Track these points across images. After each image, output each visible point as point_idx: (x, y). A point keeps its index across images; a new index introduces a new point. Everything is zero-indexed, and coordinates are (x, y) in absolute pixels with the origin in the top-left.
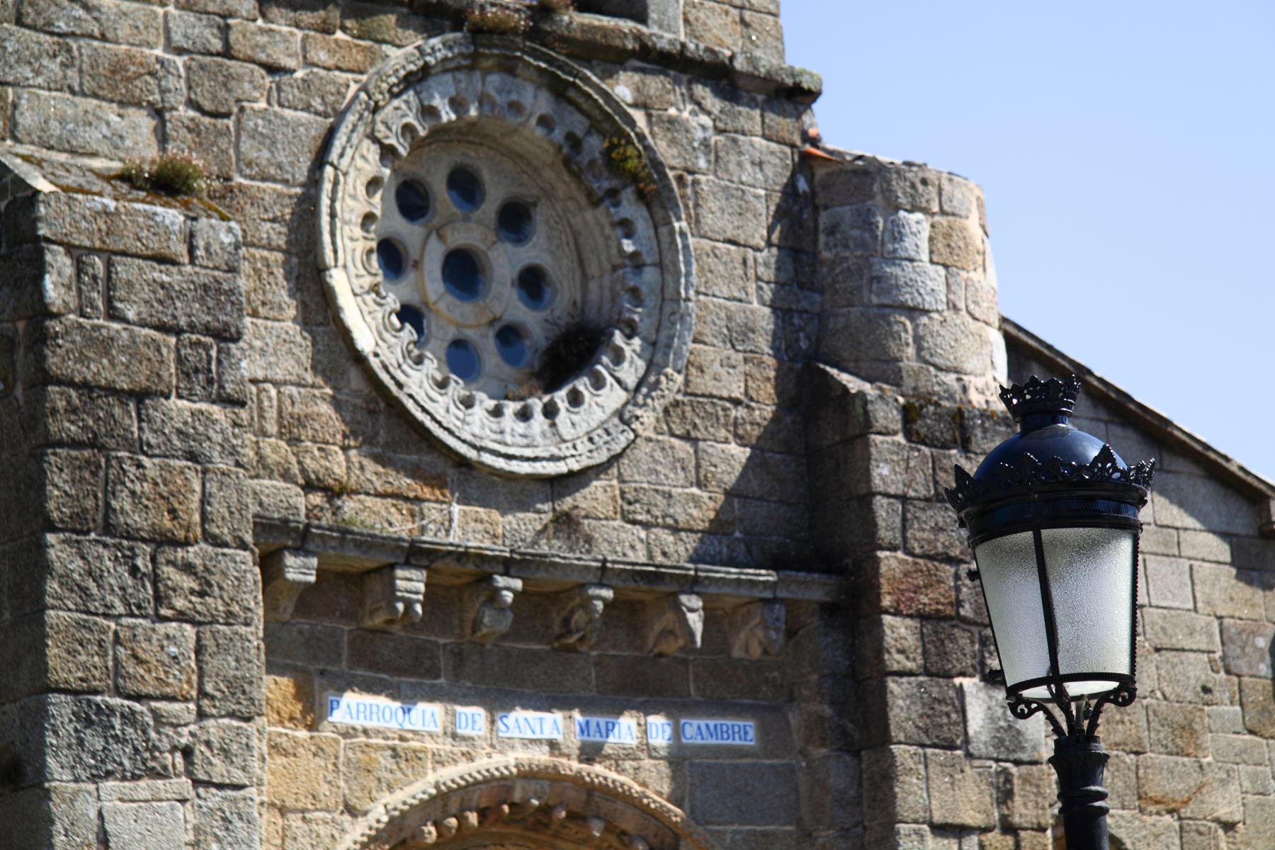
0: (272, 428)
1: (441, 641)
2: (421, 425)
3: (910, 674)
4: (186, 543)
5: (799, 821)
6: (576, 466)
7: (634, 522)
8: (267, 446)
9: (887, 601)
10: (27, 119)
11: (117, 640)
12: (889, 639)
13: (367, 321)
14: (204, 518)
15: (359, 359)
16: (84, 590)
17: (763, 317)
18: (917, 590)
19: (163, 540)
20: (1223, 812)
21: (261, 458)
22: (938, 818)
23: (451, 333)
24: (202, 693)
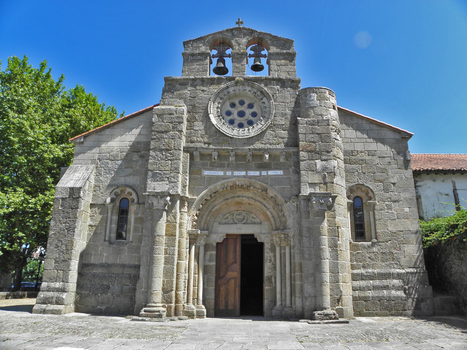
0: (199, 136)
2: (223, 133)
3: (305, 160)
4: (170, 150)
5: (291, 185)
6: (250, 136)
7: (263, 144)
8: (198, 139)
9: (301, 149)
10: (166, 102)
11: (159, 164)
12: (301, 155)
13: (214, 120)
14: (174, 147)
15: (214, 125)
16: (155, 158)
17: (289, 112)
18: (307, 147)
19: (167, 150)
20: (393, 181)
21: (197, 140)
22: (310, 182)
23: (239, 122)
24: (171, 170)
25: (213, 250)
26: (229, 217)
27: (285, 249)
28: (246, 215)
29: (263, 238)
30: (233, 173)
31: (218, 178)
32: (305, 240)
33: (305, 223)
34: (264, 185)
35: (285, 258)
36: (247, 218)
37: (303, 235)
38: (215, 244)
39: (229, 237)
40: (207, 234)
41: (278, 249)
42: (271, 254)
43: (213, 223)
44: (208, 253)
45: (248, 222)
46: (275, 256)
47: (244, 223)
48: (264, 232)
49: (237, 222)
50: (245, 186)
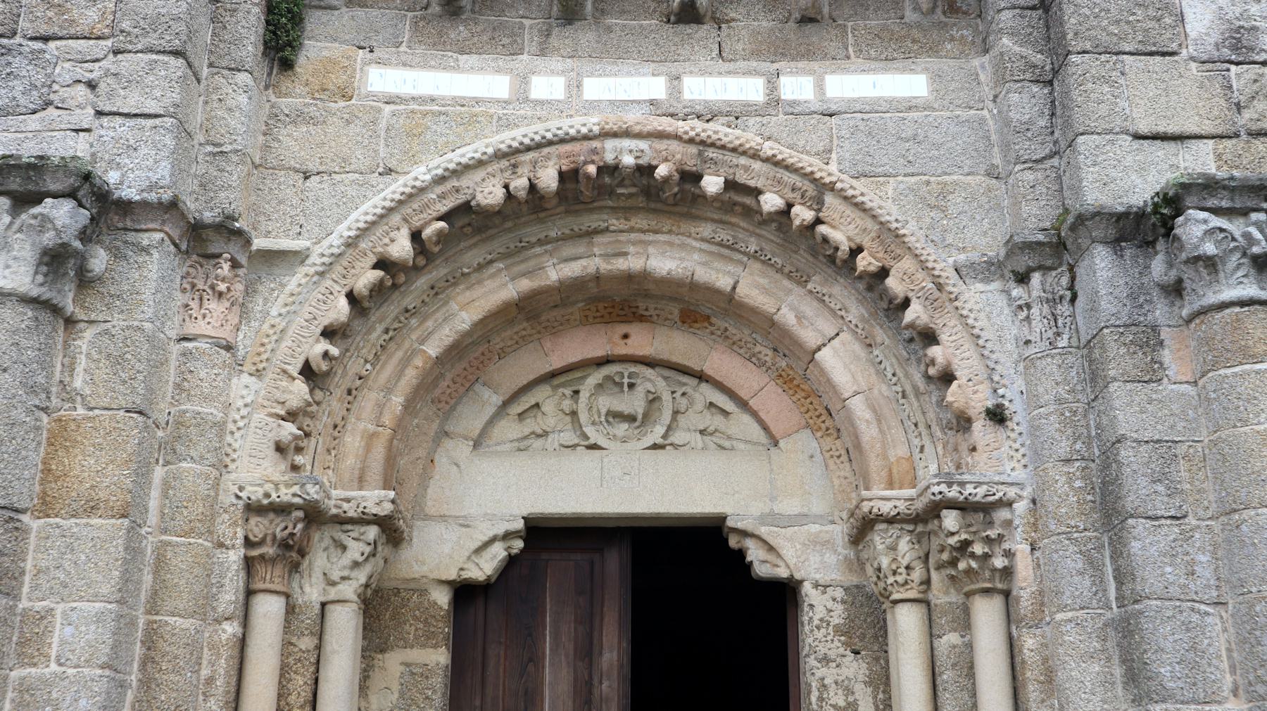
1: (527, 22)
25: (427, 640)
26: (548, 407)
27: (965, 622)
28: (666, 397)
29: (790, 552)
30: (575, 86)
31: (467, 113)
32: (1145, 543)
33: (1129, 410)
34: (810, 163)
35: (974, 695)
36: (676, 413)
37: (1130, 502)
38: (442, 598)
39: (543, 536)
40: (387, 508)
41: (907, 624)
42: (854, 669)
43: (437, 441)
44: (393, 663)
45: (677, 437)
46: (882, 681)
47: (655, 447)
48: (789, 506)
49: (602, 442)
50: (662, 171)
